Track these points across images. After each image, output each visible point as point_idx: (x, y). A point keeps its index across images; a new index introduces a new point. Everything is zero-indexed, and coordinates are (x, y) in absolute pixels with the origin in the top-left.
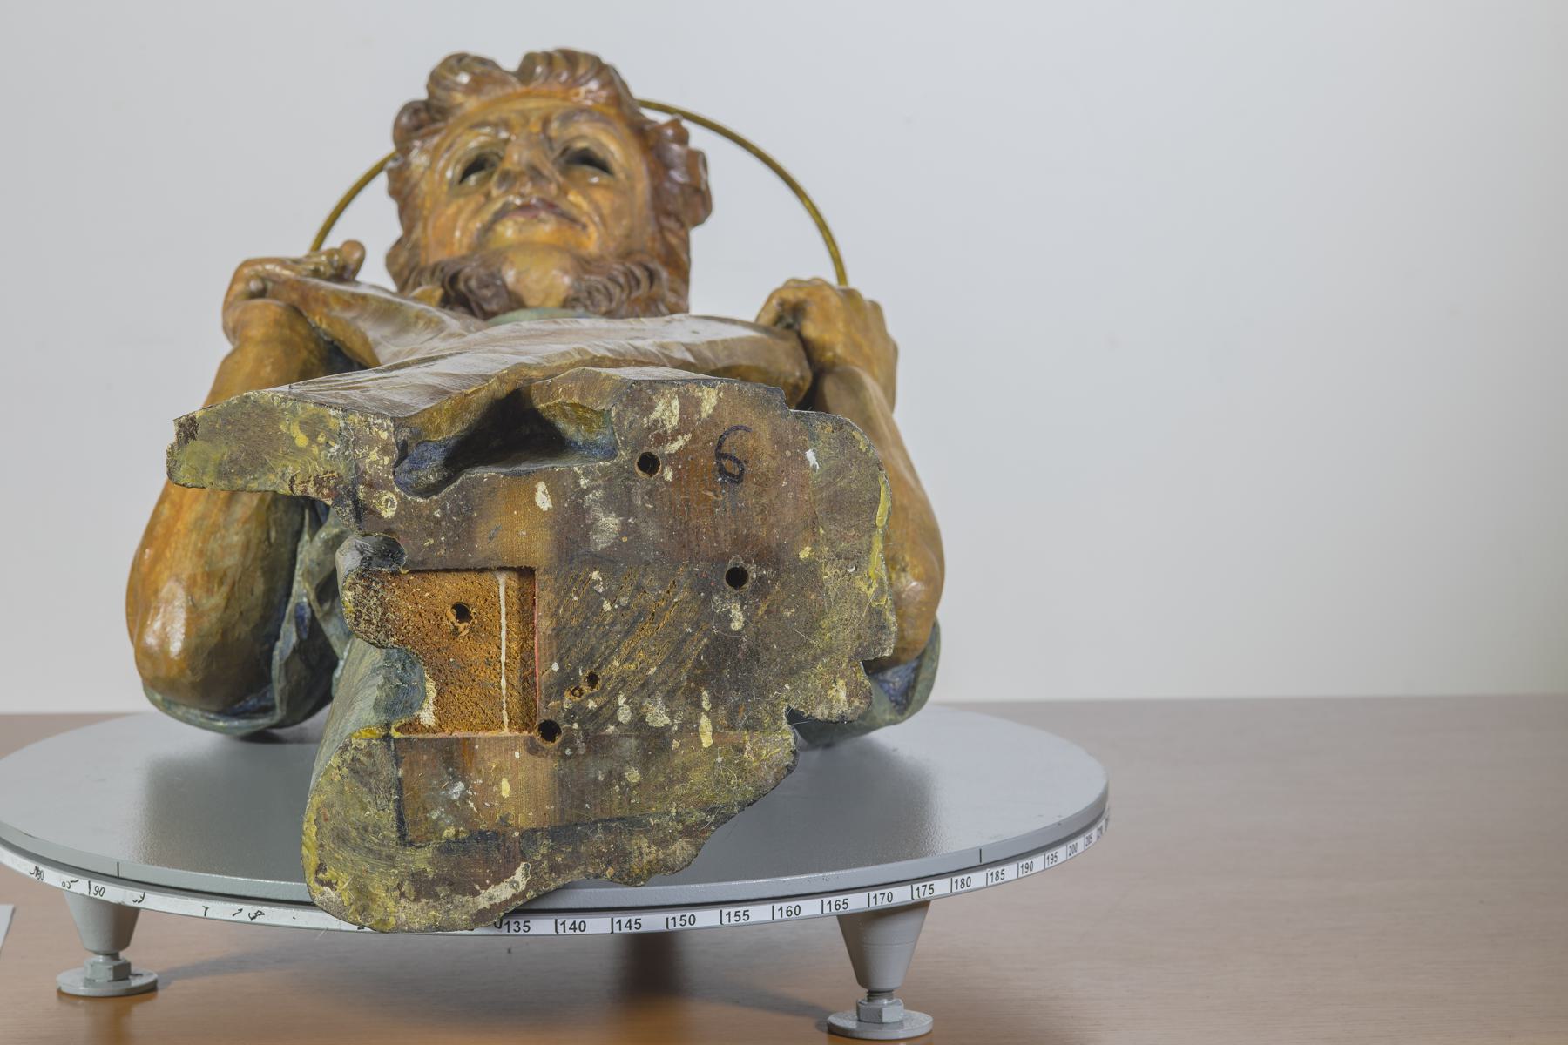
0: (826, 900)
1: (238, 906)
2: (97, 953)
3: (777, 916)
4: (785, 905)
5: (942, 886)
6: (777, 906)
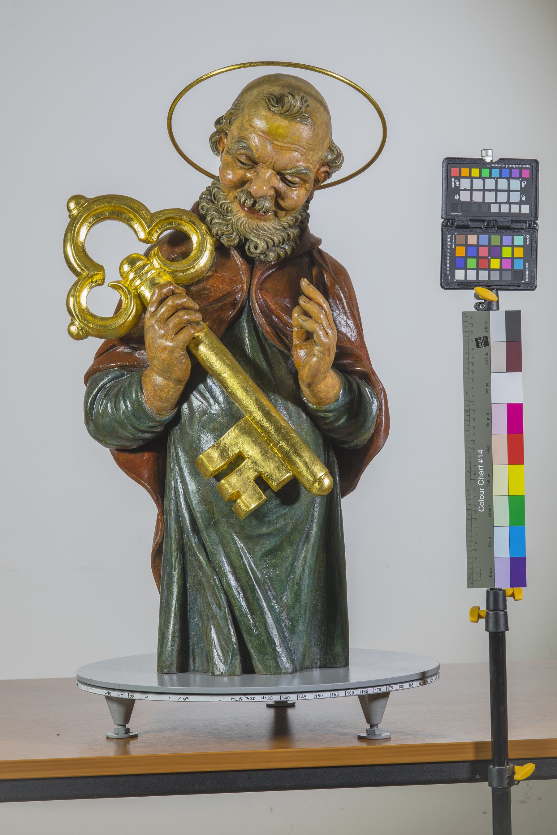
0: (361, 690)
3: (347, 694)
4: (349, 691)
5: (395, 687)
6: (347, 691)
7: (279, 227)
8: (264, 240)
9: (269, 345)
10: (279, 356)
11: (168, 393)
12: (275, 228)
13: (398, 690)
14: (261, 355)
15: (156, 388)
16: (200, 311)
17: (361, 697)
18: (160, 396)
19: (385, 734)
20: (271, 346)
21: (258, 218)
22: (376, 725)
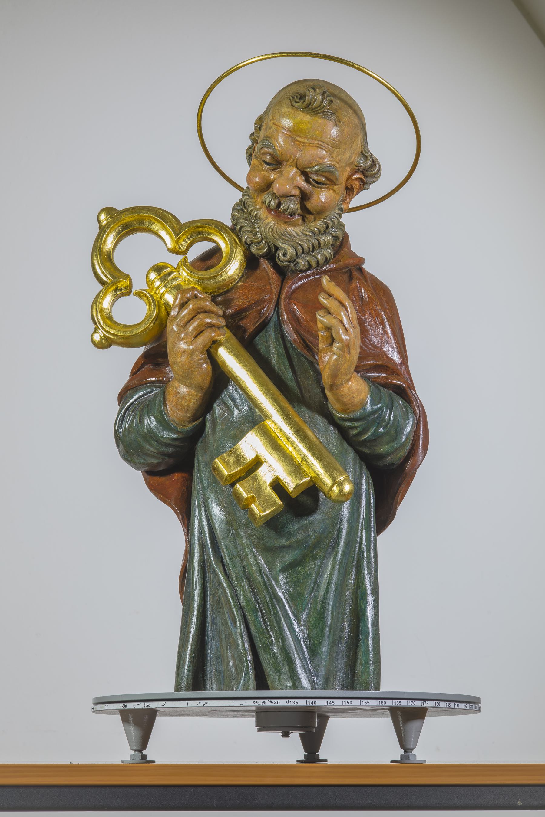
1: (199, 701)
7: (307, 233)
8: (293, 246)
9: (296, 354)
10: (307, 365)
11: (190, 401)
12: (304, 234)
14: (286, 362)
15: (178, 396)
16: (224, 316)
18: (182, 405)
20: (299, 355)
21: (286, 222)
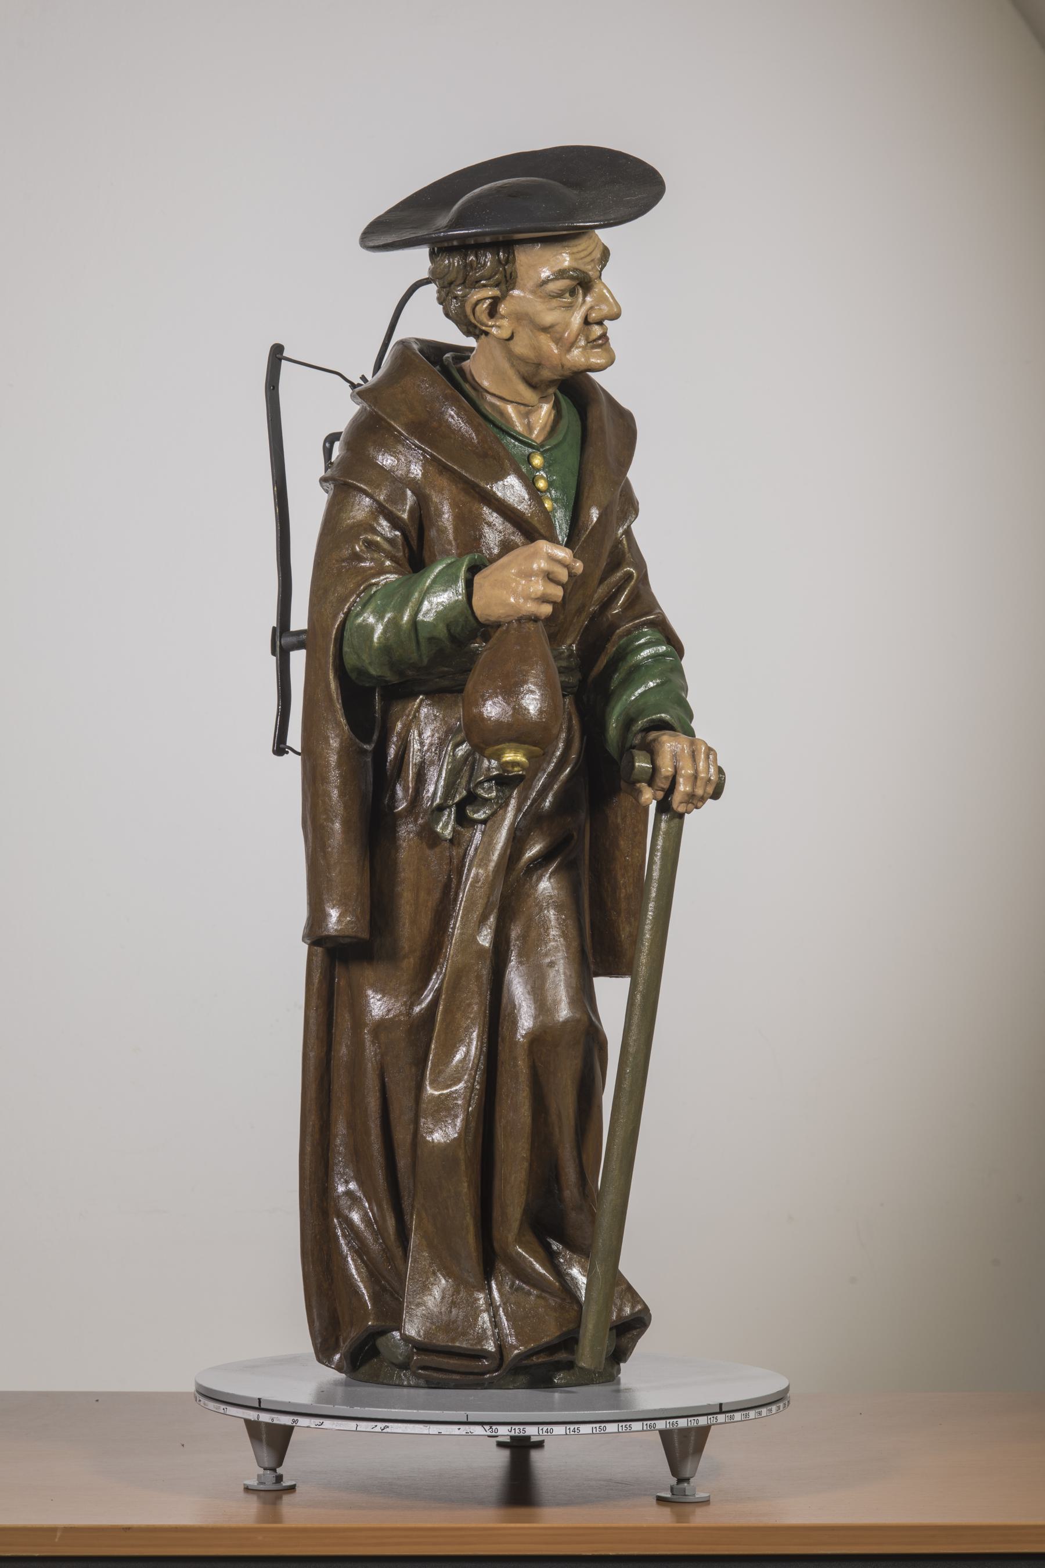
1: (373, 1424)
2: (265, 1469)
5: (721, 1418)
13: (725, 1423)
17: (664, 1434)
19: (701, 1495)
22: (687, 1480)
